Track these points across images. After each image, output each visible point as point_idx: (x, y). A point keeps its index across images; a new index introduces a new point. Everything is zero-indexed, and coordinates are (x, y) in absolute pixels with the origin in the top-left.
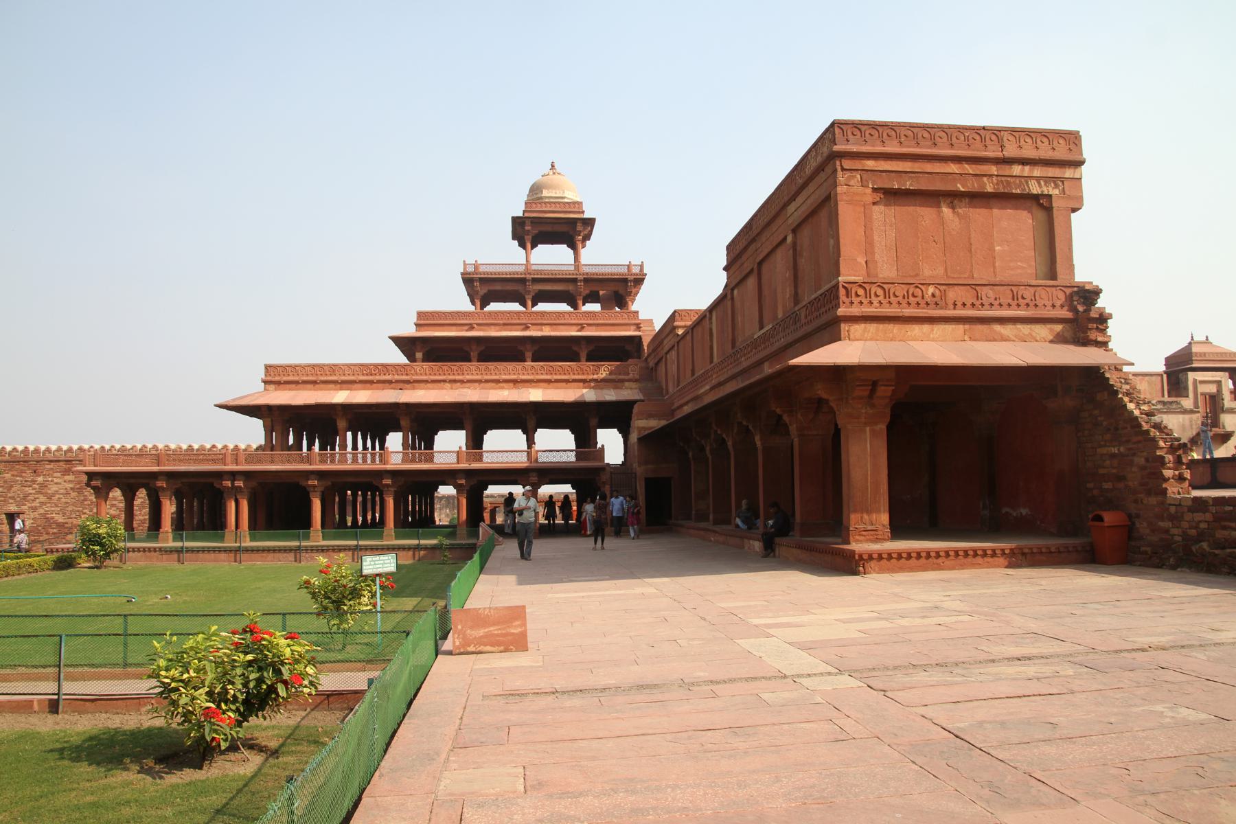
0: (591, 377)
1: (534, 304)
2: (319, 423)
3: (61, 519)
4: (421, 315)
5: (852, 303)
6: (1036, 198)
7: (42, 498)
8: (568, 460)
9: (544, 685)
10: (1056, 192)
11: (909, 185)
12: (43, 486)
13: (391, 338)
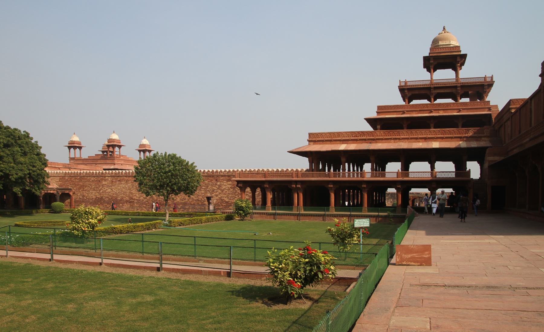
0: (464, 135)
1: (435, 100)
2: (334, 159)
3: (227, 200)
4: (379, 107)
7: (220, 191)
8: (452, 176)
9: (439, 282)
12: (220, 186)
13: (365, 119)
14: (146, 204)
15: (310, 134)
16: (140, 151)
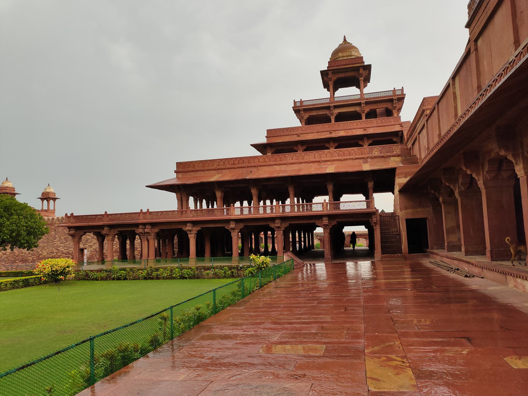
0: (367, 156)
2: (203, 191)
13: (252, 145)
14: (5, 262)
15: (179, 164)
16: (42, 199)
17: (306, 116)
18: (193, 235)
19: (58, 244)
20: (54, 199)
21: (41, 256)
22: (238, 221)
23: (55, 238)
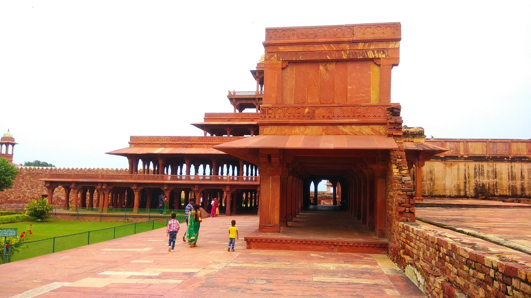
5: (265, 117)
6: (372, 60)
10: (384, 56)
11: (301, 58)
15: (132, 138)
17: (238, 103)
18: (137, 193)
19: (25, 190)
20: (13, 145)
21: (9, 199)
22: (169, 185)
23: (23, 185)
